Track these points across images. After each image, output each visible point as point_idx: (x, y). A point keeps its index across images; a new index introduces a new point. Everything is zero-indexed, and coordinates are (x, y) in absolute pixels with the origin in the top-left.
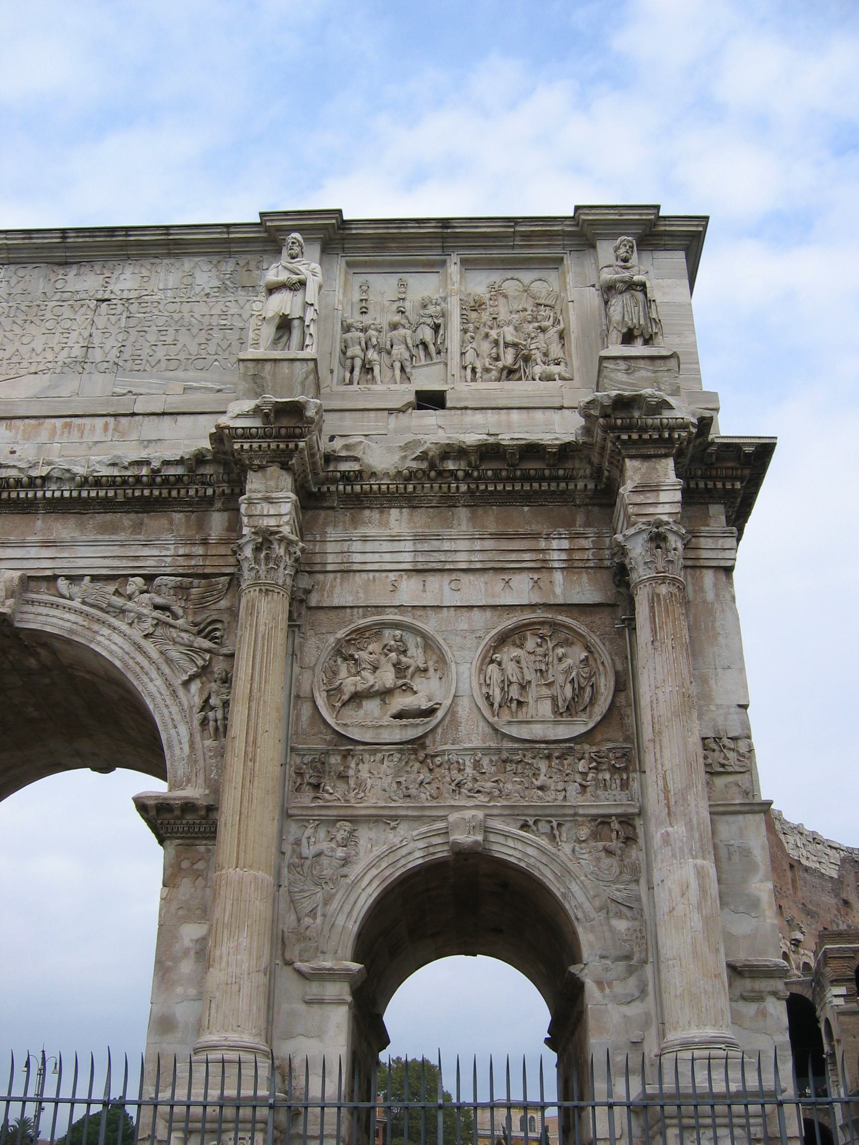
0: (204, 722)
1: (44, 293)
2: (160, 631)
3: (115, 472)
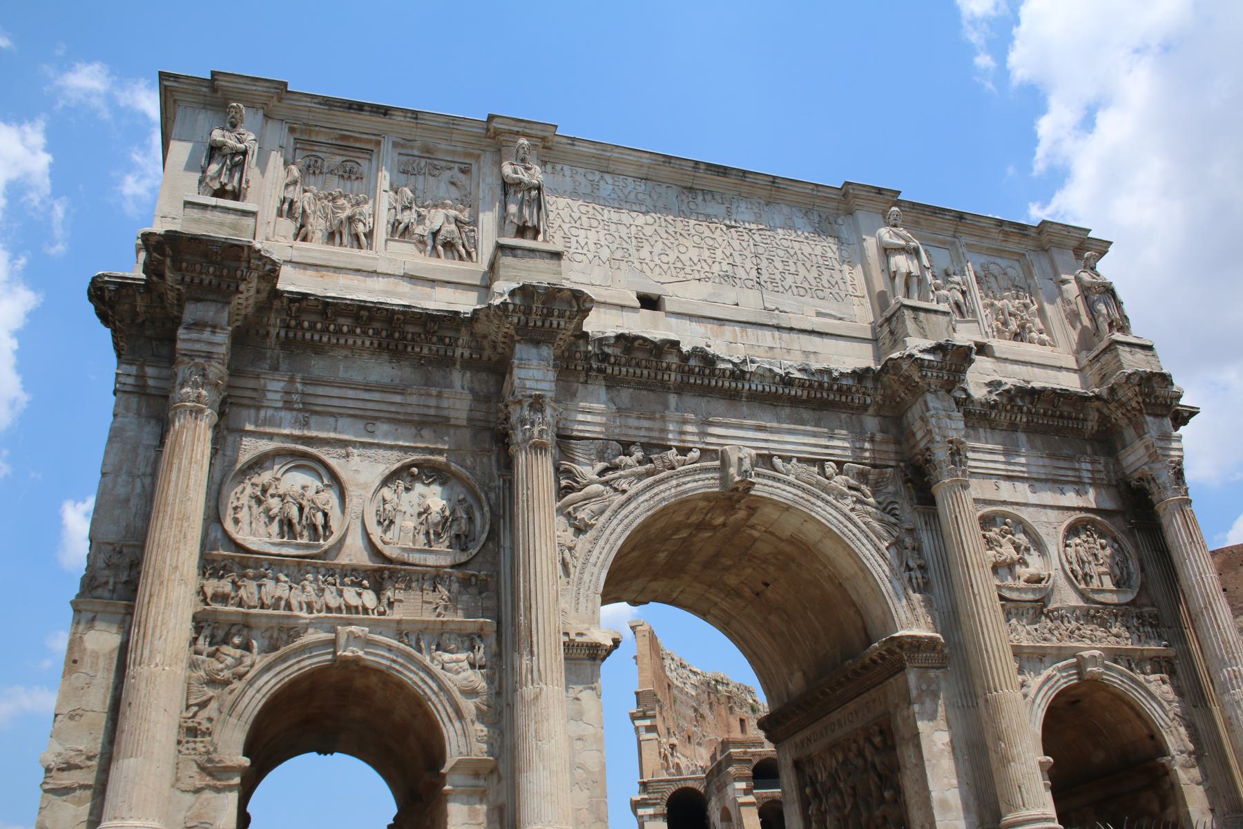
0: (910, 579)
2: (858, 506)
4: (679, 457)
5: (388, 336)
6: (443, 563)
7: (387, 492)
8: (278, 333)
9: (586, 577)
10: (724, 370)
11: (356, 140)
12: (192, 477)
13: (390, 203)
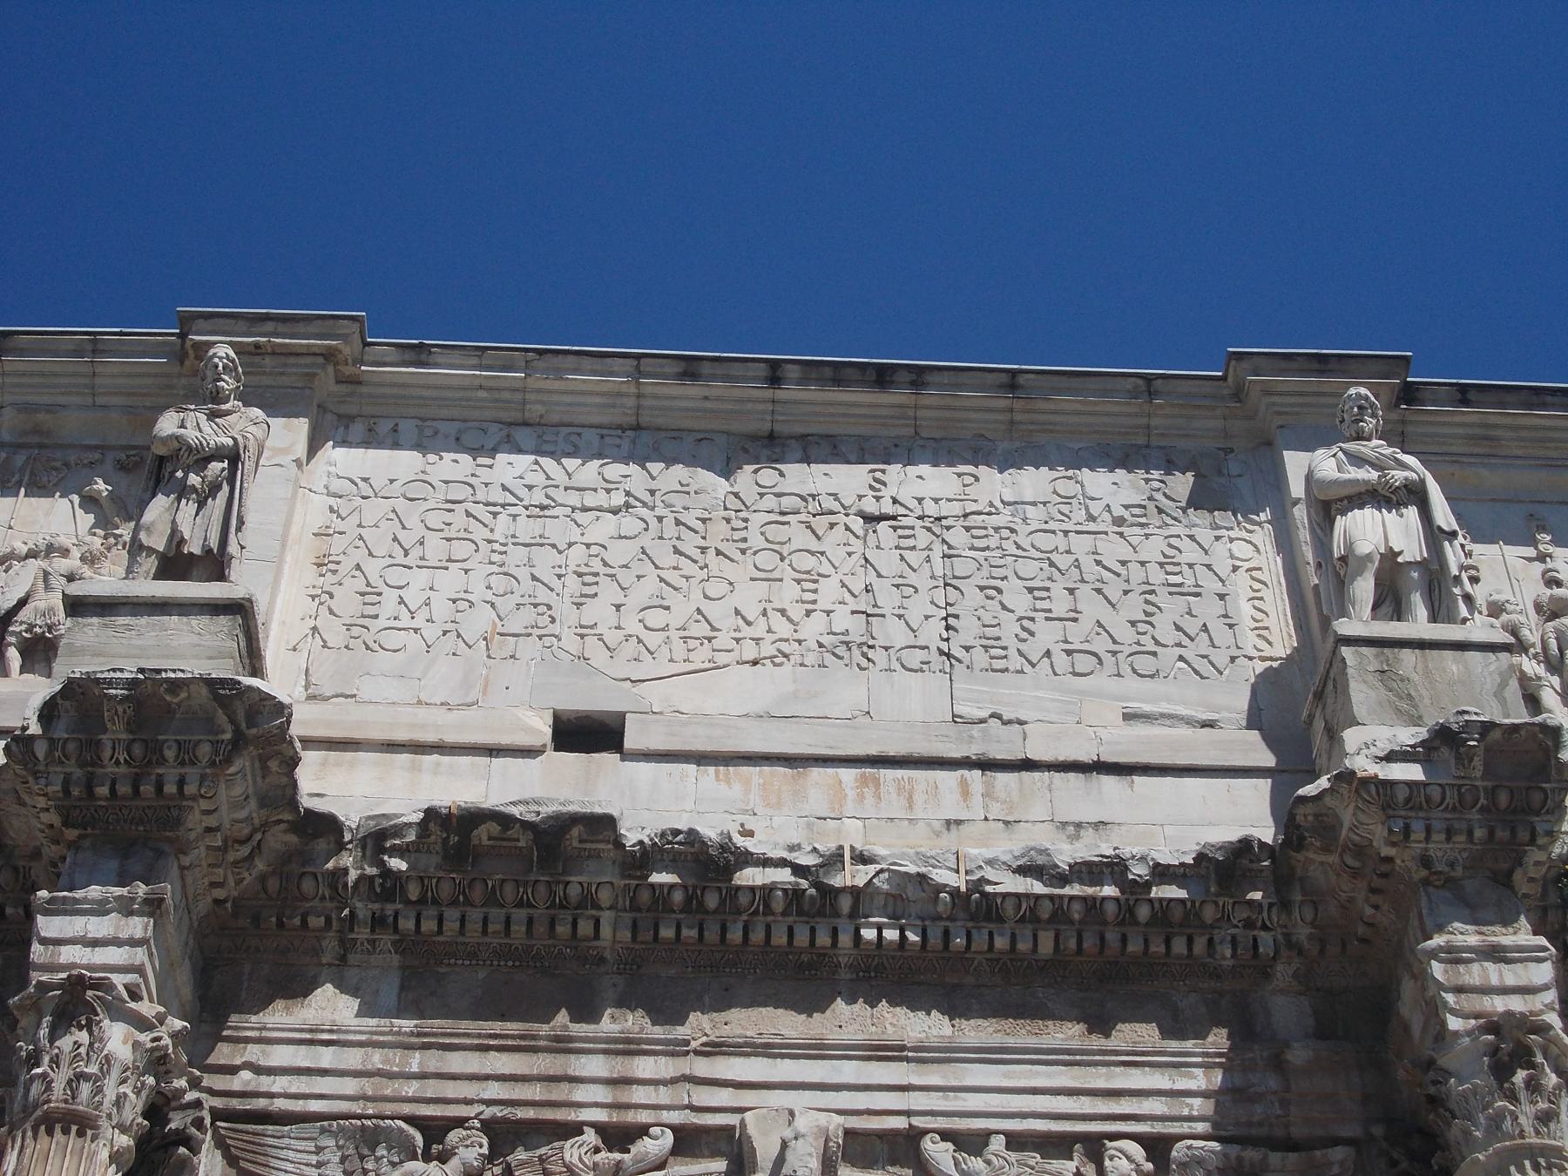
3: (1038, 888)
4: (603, 1156)
10: (768, 889)
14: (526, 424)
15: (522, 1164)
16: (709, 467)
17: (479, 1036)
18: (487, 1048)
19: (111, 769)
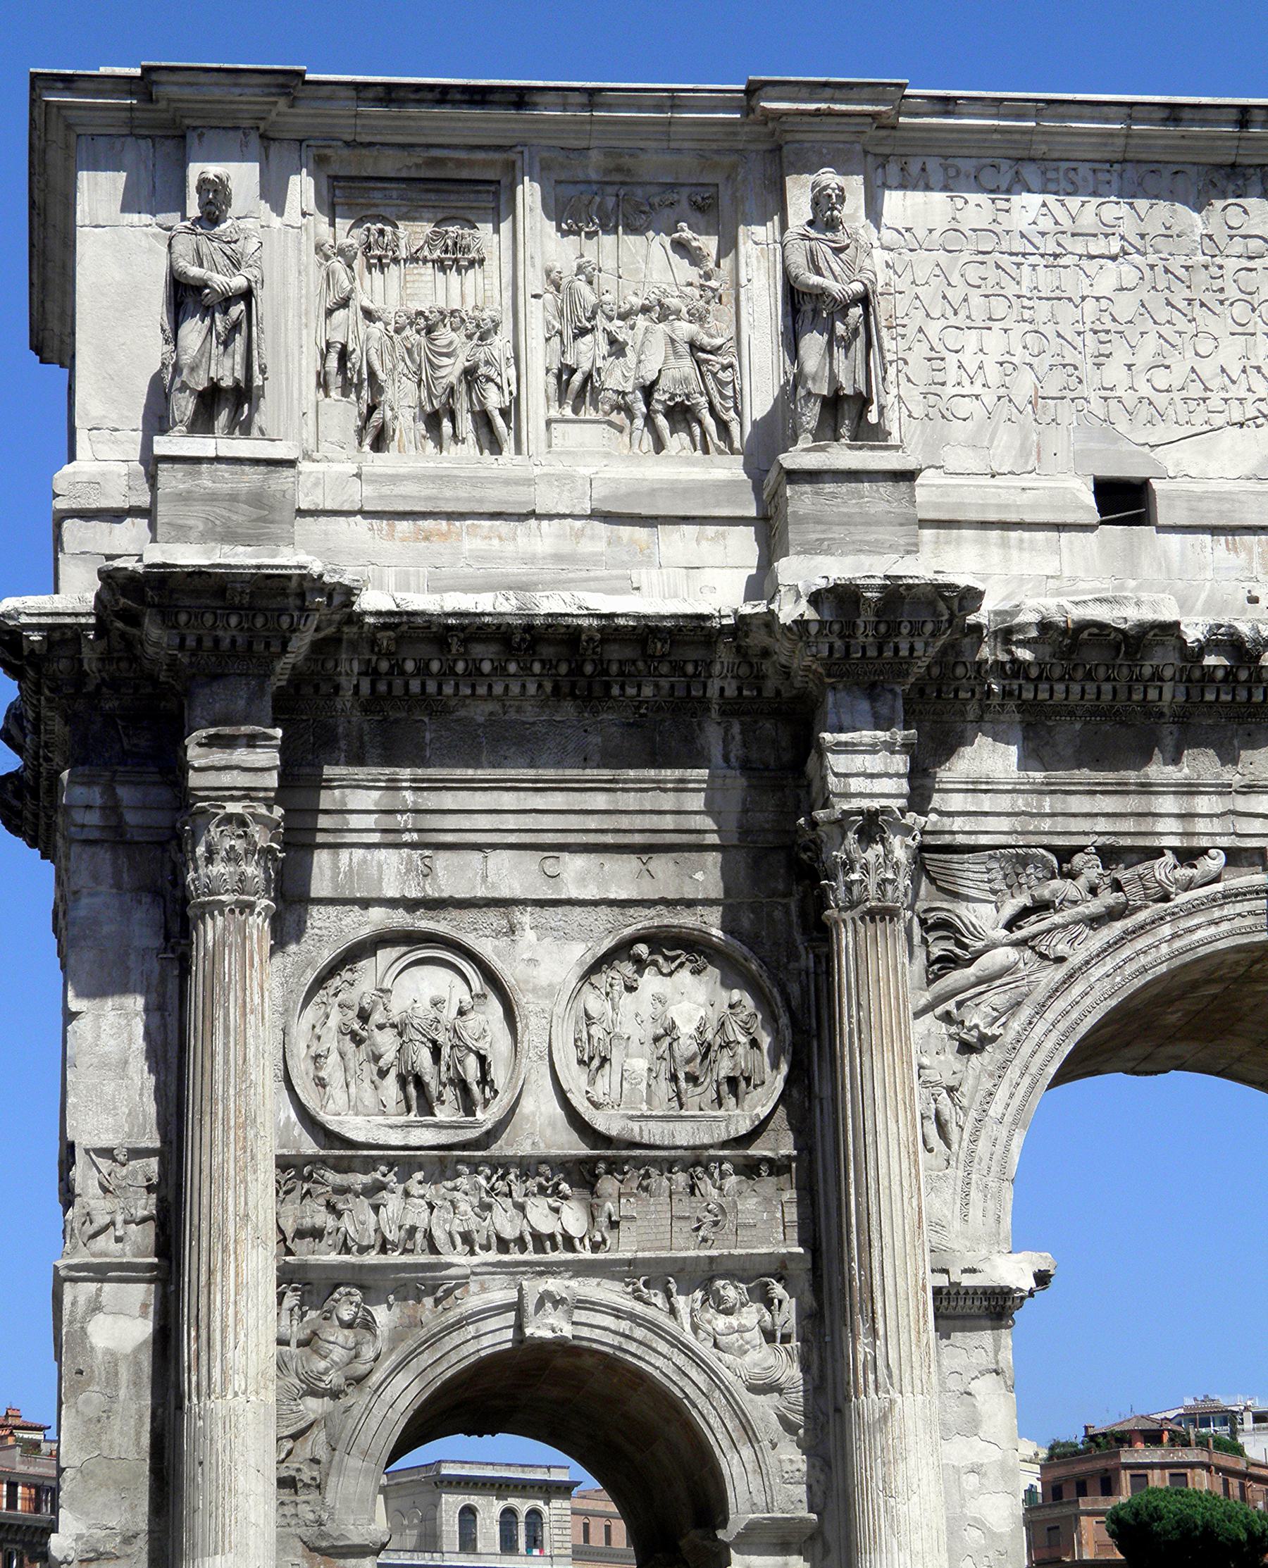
1: (1210, 237)
5: (570, 672)
6: (706, 1140)
7: (593, 1001)
8: (357, 687)
9: (983, 1146)
11: (460, 163)
12: (250, 1041)
13: (548, 323)
14: (1032, 160)
15: (1129, 881)
16: (1185, 203)
17: (1089, 784)
18: (1095, 792)
19: (862, 639)
